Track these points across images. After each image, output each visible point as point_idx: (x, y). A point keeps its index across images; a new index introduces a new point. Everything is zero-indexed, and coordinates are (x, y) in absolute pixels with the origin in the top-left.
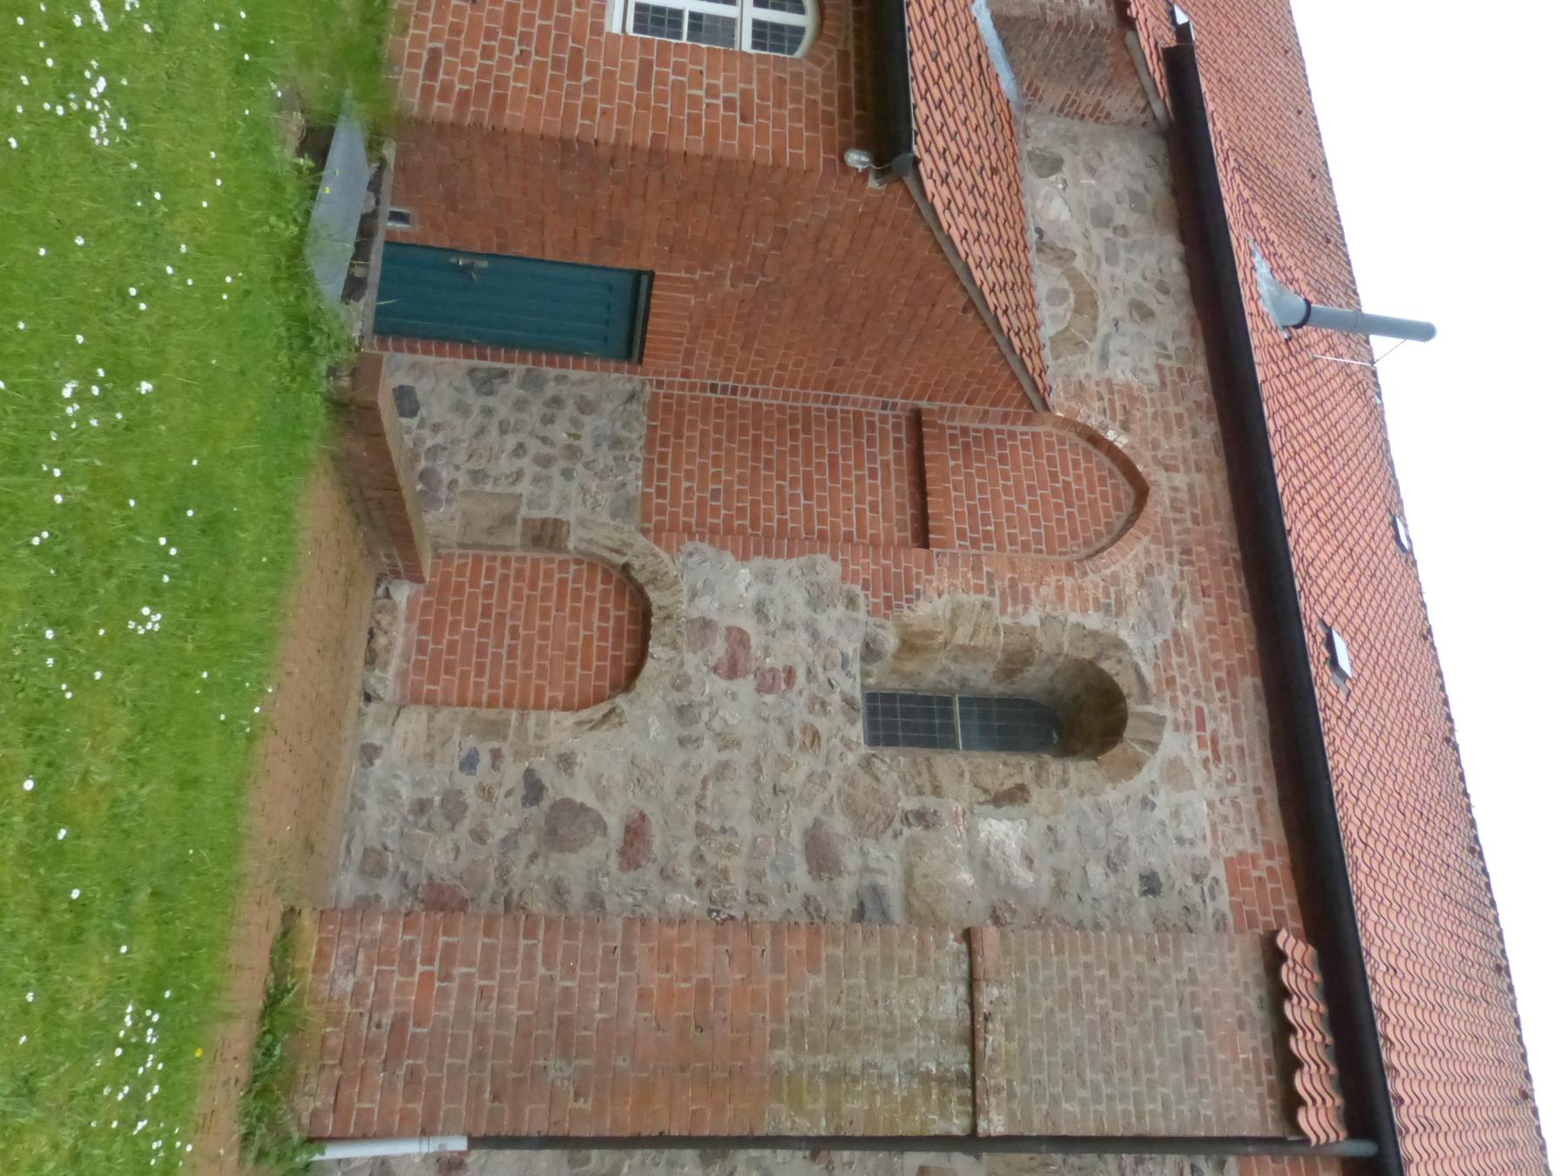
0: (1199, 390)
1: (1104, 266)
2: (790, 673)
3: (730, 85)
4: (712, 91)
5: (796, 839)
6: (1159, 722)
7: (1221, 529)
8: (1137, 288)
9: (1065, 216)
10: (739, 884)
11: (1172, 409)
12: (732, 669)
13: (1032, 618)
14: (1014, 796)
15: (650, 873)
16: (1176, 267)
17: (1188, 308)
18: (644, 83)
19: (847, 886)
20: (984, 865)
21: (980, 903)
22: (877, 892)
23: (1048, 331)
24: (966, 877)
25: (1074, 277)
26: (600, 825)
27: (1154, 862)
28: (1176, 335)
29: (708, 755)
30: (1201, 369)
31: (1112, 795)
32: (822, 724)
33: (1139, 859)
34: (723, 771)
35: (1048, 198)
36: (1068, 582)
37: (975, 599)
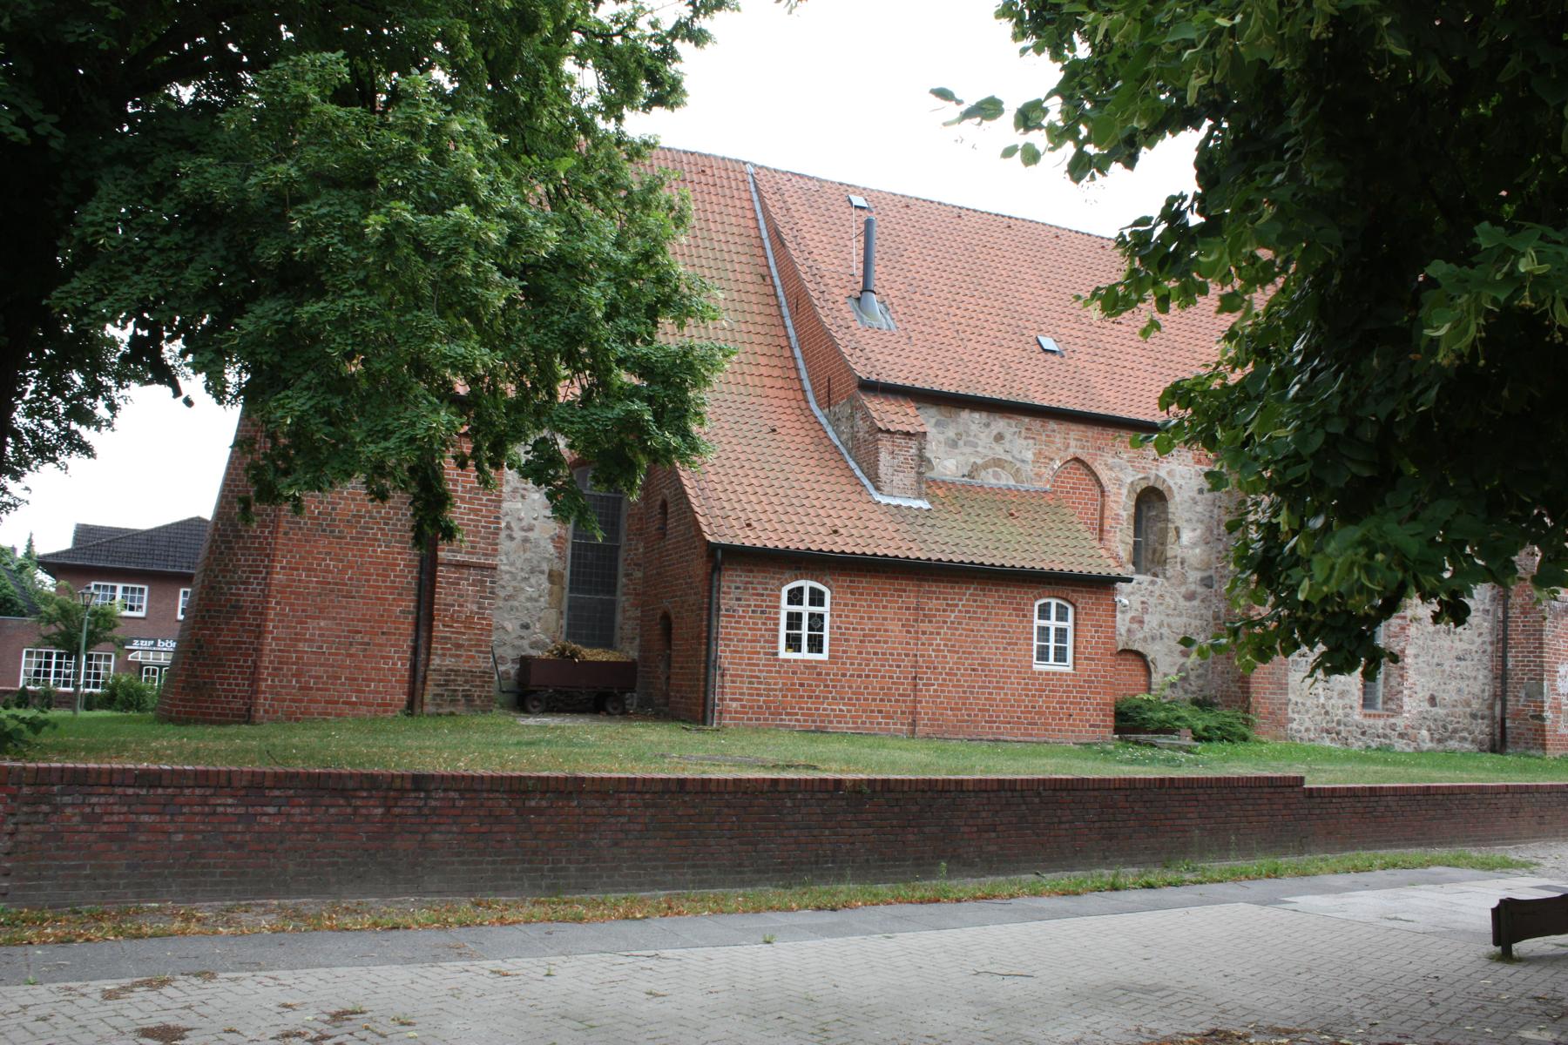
0: (1036, 424)
1: (979, 449)
2: (1143, 603)
3: (1090, 631)
4: (1092, 637)
5: (1188, 604)
6: (1157, 476)
7: (1092, 432)
8: (987, 436)
9: (954, 461)
10: (1198, 623)
11: (1044, 438)
12: (1141, 622)
13: (1124, 514)
14: (1177, 530)
16: (976, 415)
17: (997, 416)
18: (1093, 659)
19: (1200, 589)
20: (1194, 545)
21: (1204, 547)
22: (1202, 579)
23: (1012, 483)
24: (1197, 551)
25: (986, 466)
27: (1196, 488)
28: (1009, 425)
29: (1165, 630)
30: (1027, 420)
31: (1178, 498)
32: (1157, 593)
33: (1194, 494)
34: (1169, 626)
35: (945, 467)
36: (1112, 498)
37: (1118, 534)
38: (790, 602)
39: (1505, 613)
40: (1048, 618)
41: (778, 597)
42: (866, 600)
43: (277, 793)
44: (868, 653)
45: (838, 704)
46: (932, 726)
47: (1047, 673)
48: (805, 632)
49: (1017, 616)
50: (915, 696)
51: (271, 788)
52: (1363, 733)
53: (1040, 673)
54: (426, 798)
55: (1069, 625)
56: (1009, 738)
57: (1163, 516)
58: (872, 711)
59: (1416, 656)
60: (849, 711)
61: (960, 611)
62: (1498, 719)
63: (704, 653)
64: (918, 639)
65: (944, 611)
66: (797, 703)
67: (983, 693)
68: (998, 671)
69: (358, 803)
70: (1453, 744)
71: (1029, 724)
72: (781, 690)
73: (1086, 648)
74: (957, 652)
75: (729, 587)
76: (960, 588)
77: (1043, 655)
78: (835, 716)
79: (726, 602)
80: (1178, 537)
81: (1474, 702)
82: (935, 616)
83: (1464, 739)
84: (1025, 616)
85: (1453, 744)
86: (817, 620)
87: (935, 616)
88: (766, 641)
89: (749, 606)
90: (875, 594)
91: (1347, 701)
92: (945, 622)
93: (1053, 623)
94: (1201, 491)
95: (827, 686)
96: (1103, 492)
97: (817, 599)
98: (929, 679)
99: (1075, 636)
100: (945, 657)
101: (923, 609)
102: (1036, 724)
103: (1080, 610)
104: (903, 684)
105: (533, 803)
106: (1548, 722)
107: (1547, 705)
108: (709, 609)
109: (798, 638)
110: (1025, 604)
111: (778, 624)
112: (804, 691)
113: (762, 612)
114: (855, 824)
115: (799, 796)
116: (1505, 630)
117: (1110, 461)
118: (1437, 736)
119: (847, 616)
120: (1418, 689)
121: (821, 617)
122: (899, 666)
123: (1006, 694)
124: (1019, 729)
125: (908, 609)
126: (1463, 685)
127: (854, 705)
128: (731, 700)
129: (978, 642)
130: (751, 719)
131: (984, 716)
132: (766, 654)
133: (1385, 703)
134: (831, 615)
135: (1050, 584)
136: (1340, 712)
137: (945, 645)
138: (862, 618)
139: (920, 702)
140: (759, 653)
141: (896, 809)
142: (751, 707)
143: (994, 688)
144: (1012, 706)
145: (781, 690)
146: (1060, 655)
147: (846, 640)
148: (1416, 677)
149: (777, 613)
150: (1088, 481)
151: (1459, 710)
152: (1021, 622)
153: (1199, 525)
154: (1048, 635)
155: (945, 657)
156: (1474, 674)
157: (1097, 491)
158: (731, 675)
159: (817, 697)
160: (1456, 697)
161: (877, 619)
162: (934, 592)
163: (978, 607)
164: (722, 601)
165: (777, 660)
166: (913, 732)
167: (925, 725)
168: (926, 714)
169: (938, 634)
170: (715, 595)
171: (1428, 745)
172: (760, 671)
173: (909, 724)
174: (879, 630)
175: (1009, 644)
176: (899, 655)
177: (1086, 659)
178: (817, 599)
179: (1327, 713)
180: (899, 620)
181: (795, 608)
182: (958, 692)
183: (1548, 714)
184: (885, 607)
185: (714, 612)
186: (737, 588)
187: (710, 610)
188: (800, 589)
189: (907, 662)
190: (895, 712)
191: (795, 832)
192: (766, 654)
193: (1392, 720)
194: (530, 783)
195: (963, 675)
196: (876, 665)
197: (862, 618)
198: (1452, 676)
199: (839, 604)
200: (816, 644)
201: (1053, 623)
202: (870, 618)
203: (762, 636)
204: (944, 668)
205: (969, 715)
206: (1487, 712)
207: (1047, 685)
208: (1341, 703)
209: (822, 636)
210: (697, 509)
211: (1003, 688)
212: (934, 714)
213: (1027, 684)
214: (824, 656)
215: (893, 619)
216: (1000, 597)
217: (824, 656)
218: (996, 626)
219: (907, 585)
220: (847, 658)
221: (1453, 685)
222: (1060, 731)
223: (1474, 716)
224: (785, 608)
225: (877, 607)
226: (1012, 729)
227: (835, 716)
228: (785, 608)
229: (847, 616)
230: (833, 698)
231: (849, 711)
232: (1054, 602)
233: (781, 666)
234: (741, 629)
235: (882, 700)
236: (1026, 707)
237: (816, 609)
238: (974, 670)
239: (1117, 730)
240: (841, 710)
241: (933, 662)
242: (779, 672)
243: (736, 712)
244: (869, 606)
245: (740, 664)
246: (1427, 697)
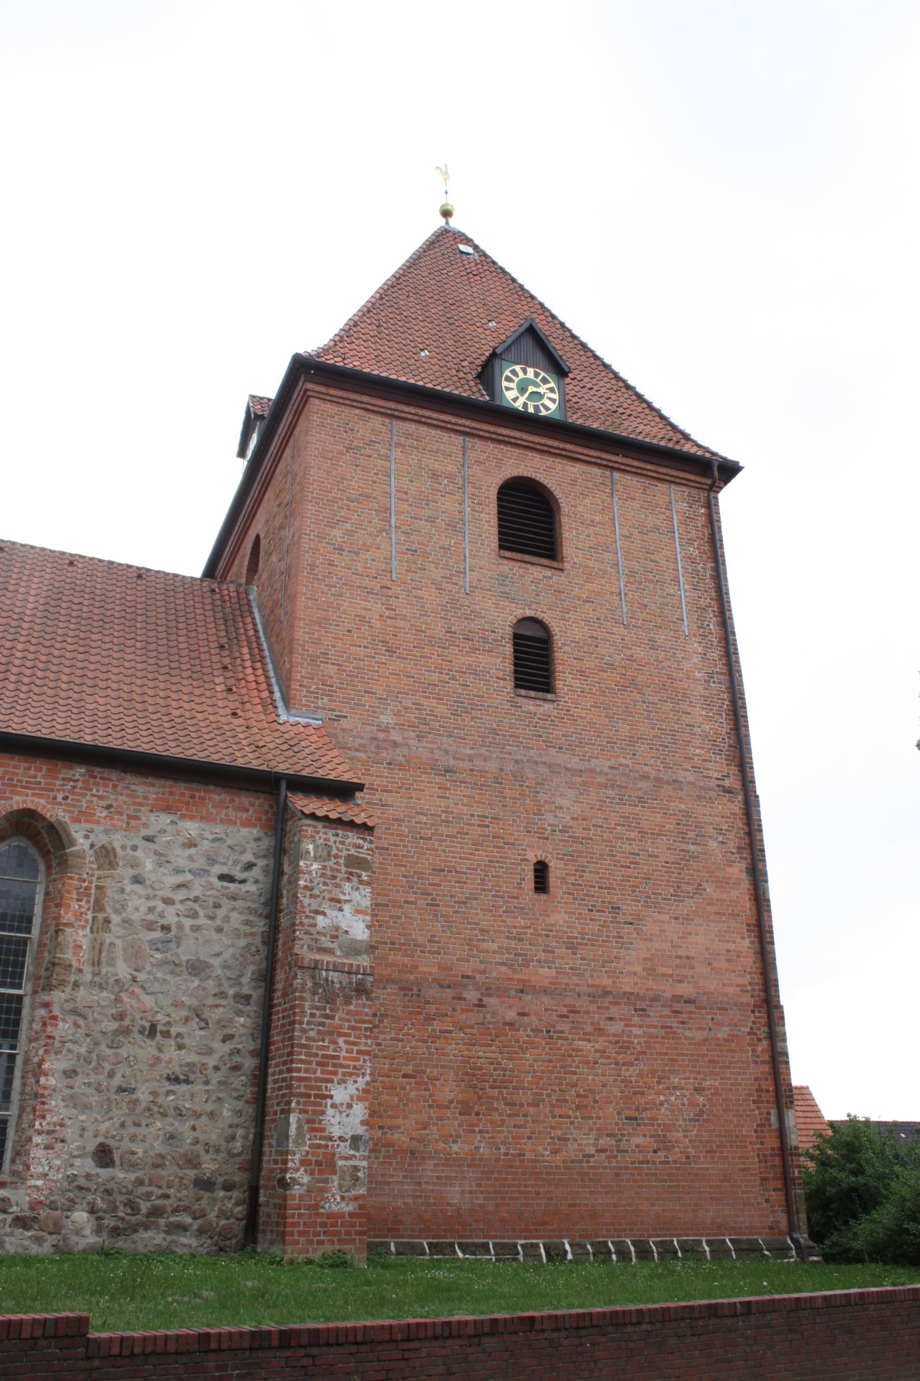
59: (70, 1074)
81: (205, 1158)
83: (183, 1228)
107: (294, 1161)
118: (109, 1222)
120: (69, 1133)
126: (183, 1128)
148: (64, 1112)
151: (170, 1172)
156: (209, 1107)
198: (155, 1110)
206: (240, 1177)
246: (92, 1146)
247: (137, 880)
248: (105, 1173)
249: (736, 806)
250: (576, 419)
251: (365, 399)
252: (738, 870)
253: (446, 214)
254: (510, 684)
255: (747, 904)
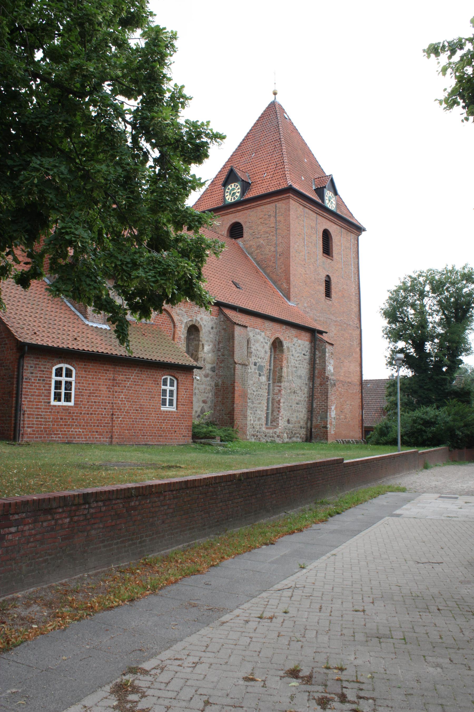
5: (205, 379)
6: (196, 320)
13: (183, 336)
14: (203, 345)
15: (208, 400)
18: (184, 405)
19: (210, 373)
20: (209, 352)
22: (211, 368)
24: (210, 355)
26: (203, 407)
31: (204, 331)
33: (210, 329)
34: (198, 389)
36: (178, 329)
38: (56, 375)
39: (313, 385)
40: (166, 385)
41: (51, 372)
42: (91, 375)
43: (16, 517)
44: (92, 402)
45: (78, 429)
46: (119, 438)
47: (167, 412)
48: (63, 391)
49: (155, 384)
50: (112, 423)
51: (13, 514)
52: (266, 436)
53: (164, 412)
54: (90, 507)
55: (174, 388)
56: (151, 443)
57: (197, 338)
58: (93, 432)
59: (284, 403)
60: (83, 432)
61: (131, 381)
62: (309, 428)
63: (14, 402)
64: (114, 395)
65: (125, 381)
66: (59, 428)
67: (141, 422)
68: (147, 411)
69: (58, 517)
70: (294, 439)
71: (159, 436)
72: (52, 422)
73: (182, 399)
74: (130, 402)
75: (27, 367)
76: (132, 370)
77: (164, 403)
78: (77, 435)
79: (26, 374)
80: (203, 348)
82: (121, 383)
83: (298, 437)
84: (158, 384)
85: (294, 439)
86: (68, 384)
87: (121, 383)
88: (45, 396)
89: (37, 377)
90: (96, 372)
91: (260, 422)
92: (125, 387)
93: (168, 388)
94: (212, 328)
95: (73, 419)
96: (174, 326)
97: (69, 374)
98: (118, 415)
99: (177, 394)
100: (125, 404)
101: (116, 380)
102: (161, 436)
103: (179, 381)
104: (107, 418)
105: (133, 504)
106: (328, 429)
108: (18, 378)
109: (60, 394)
110: (158, 378)
111: (50, 387)
112: (63, 422)
113: (44, 380)
114: (238, 497)
115: (223, 485)
116: (313, 392)
117: (178, 311)
119: (83, 383)
120: (284, 416)
121: (71, 383)
122: (105, 409)
123: (150, 422)
124: (155, 439)
125: (109, 380)
127: (85, 429)
128: (28, 427)
129: (139, 397)
130: (37, 438)
131: (141, 433)
132: (45, 402)
133: (271, 423)
134: (76, 382)
135: (168, 369)
136: (258, 427)
137: (125, 398)
138: (89, 384)
139: (114, 426)
140: (41, 402)
141: (249, 487)
142: (37, 431)
143: (146, 419)
144: (152, 428)
145: (52, 422)
146: (171, 404)
147: (82, 395)
149: (50, 381)
150: (169, 320)
151: (297, 425)
152: (156, 387)
153: (211, 343)
154: (166, 393)
155: (125, 404)
157: (172, 325)
158: (28, 414)
159: (69, 425)
160: (296, 420)
161: (96, 384)
162: (121, 372)
163: (139, 379)
164: (24, 374)
165: (50, 406)
166: (111, 442)
167: (116, 438)
168: (117, 432)
169: (122, 392)
170: (21, 371)
171: (286, 440)
172: (42, 412)
173: (110, 438)
174: (97, 390)
175: (151, 397)
176: (105, 403)
177: (182, 405)
178: (69, 374)
179: (254, 427)
180: (106, 385)
181: (59, 378)
182: (130, 421)
183: (328, 426)
184: (99, 379)
185: (20, 380)
186: (31, 367)
187: (19, 379)
188: (61, 369)
189: (109, 406)
190: (103, 432)
191: (221, 504)
192: (45, 402)
193: (275, 430)
194: (133, 491)
195: (132, 413)
196: (95, 408)
197: (89, 384)
199: (79, 377)
200: (68, 398)
201: (168, 388)
202: (93, 384)
203: (43, 393)
204: (124, 409)
205: (135, 433)
206: (305, 426)
207: (167, 417)
208: (258, 423)
209: (71, 393)
210: (7, 323)
211: (149, 419)
212: (120, 432)
213: (158, 417)
214: (72, 404)
215: (103, 385)
216: (148, 375)
217: (72, 404)
218: (146, 389)
219: (109, 368)
220: (83, 405)
221: (295, 414)
222: (171, 439)
223: (301, 427)
224: (54, 378)
225: (96, 378)
226: (152, 438)
227: (77, 435)
228: (54, 378)
229: (83, 383)
230: (76, 426)
231: (83, 432)
232: (169, 377)
233: (52, 409)
234: (33, 389)
235: (98, 426)
236: (158, 428)
237: (69, 379)
238: (137, 410)
239: (193, 438)
240: (79, 432)
241: (120, 407)
242: (50, 412)
243: (30, 434)
244: (93, 378)
245: (32, 408)
247: (293, 355)
248: (289, 425)
249: (359, 332)
250: (339, 213)
251: (300, 200)
252: (358, 349)
253: (275, 94)
254: (324, 295)
255: (359, 359)
